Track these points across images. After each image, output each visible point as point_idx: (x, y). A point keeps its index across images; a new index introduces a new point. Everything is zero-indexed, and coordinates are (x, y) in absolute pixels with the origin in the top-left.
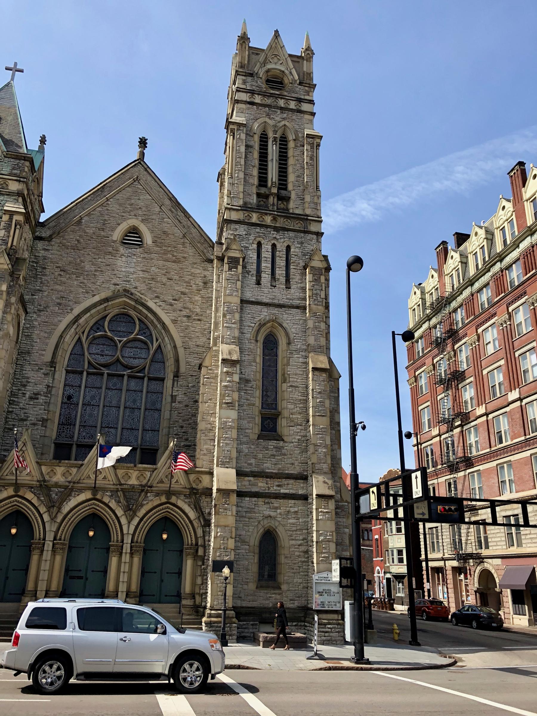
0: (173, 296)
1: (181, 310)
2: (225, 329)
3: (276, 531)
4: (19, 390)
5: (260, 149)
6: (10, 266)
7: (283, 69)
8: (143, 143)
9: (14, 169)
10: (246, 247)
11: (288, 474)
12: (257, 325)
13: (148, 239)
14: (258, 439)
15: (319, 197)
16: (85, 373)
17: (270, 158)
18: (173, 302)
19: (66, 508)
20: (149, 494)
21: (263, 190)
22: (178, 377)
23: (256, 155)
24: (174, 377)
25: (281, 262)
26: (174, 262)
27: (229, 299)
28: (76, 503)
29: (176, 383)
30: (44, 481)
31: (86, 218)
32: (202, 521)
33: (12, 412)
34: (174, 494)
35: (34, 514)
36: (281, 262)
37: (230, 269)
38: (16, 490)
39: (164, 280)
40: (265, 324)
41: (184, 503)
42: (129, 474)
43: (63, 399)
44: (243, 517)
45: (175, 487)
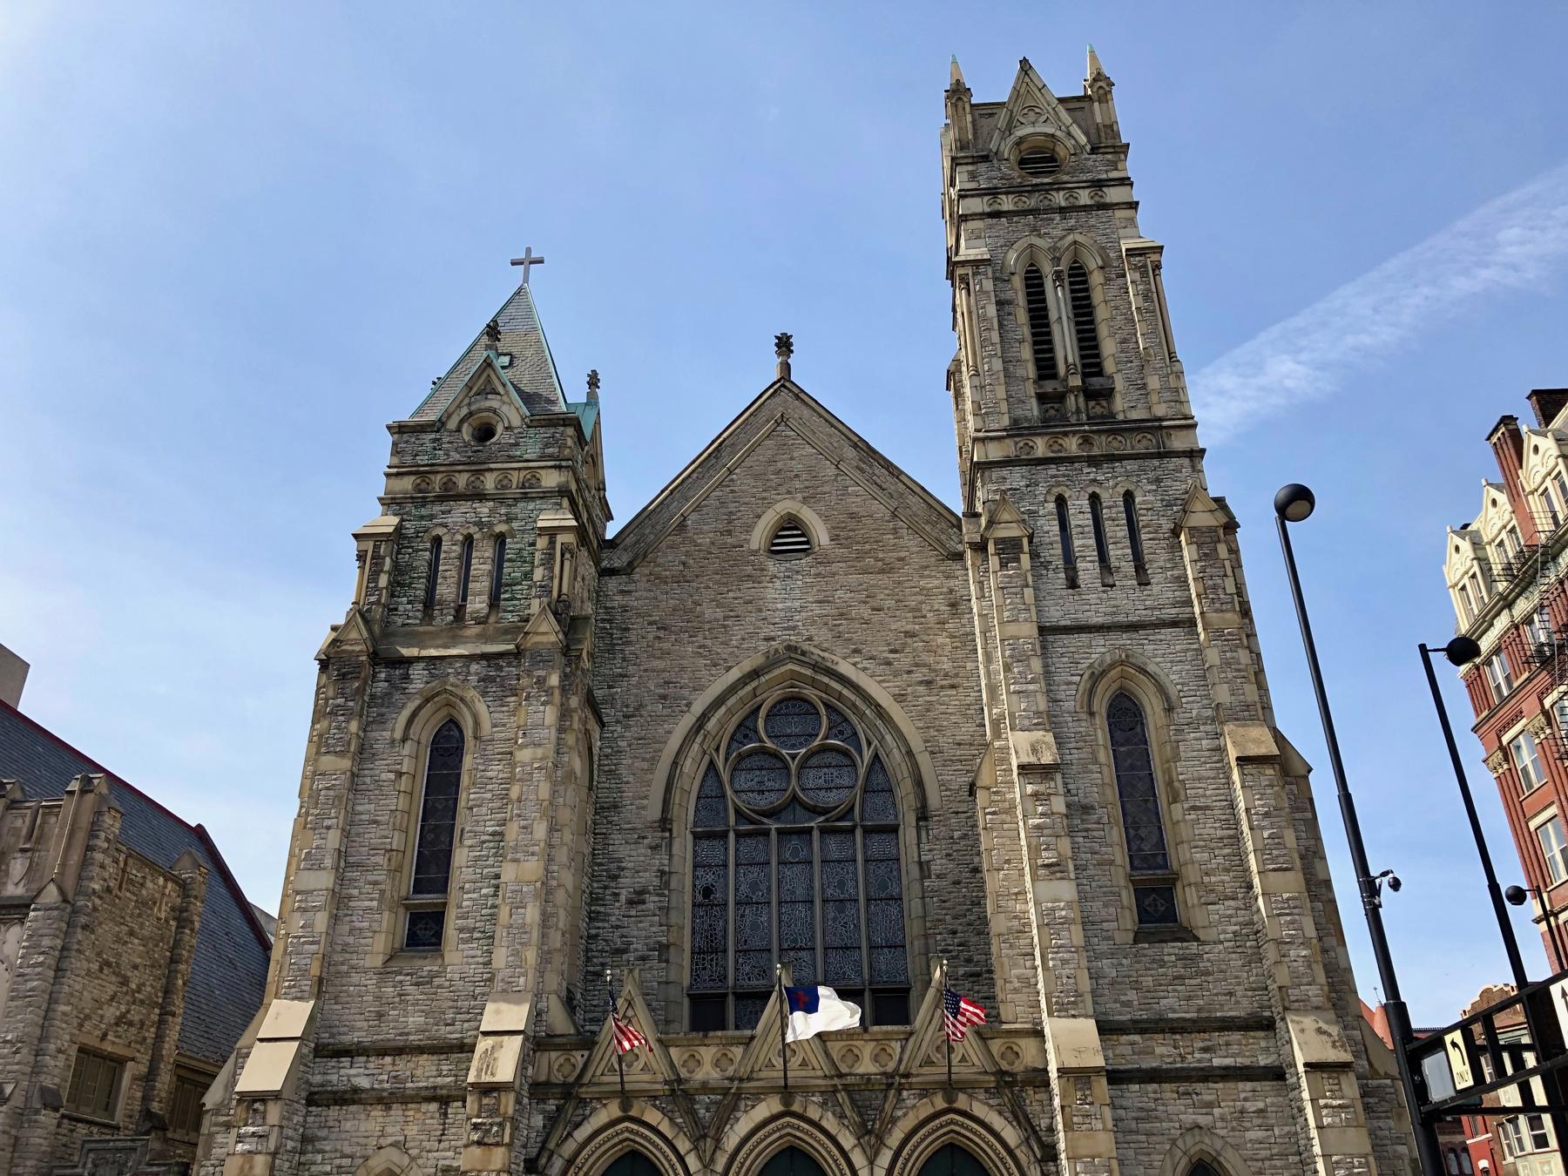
1: (909, 672)
2: (1015, 697)
3: (1219, 1163)
4: (606, 887)
5: (1029, 302)
6: (561, 636)
7: (1050, 130)
8: (784, 344)
9: (547, 446)
10: (1030, 512)
11: (1223, 1019)
12: (1086, 677)
13: (821, 534)
14: (1136, 941)
15: (1179, 374)
16: (732, 835)
17: (1053, 315)
19: (731, 1140)
20: (905, 1093)
21: (1049, 387)
22: (926, 819)
23: (1022, 316)
24: (918, 819)
25: (1116, 531)
26: (882, 571)
27: (1012, 629)
28: (752, 1125)
30: (679, 1081)
31: (694, 517)
33: (597, 935)
34: (960, 1090)
35: (666, 1157)
36: (1116, 531)
37: (1003, 565)
38: (625, 1106)
39: (865, 612)
40: (1103, 673)
42: (856, 1051)
43: (694, 897)
44: (1131, 1132)
45: (961, 1072)
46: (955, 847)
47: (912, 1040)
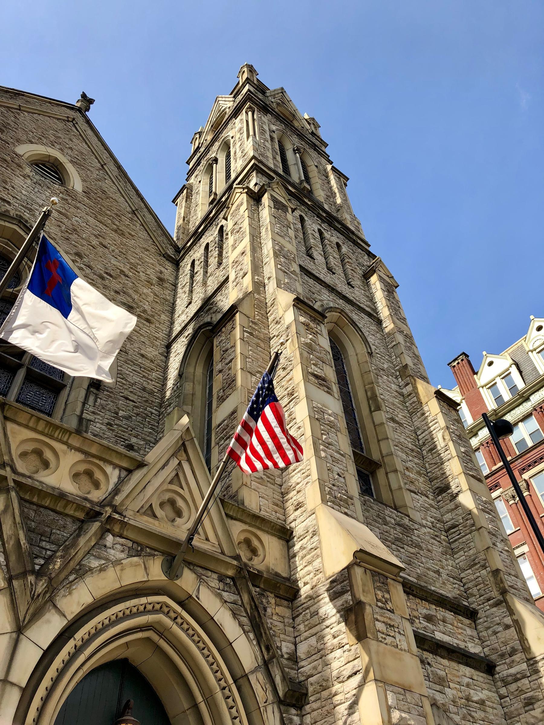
0: (106, 269)
18: (105, 275)
20: (110, 539)
29: (91, 399)
32: (278, 680)
34: (189, 564)
41: (217, 603)
46: (117, 422)
47: (137, 476)
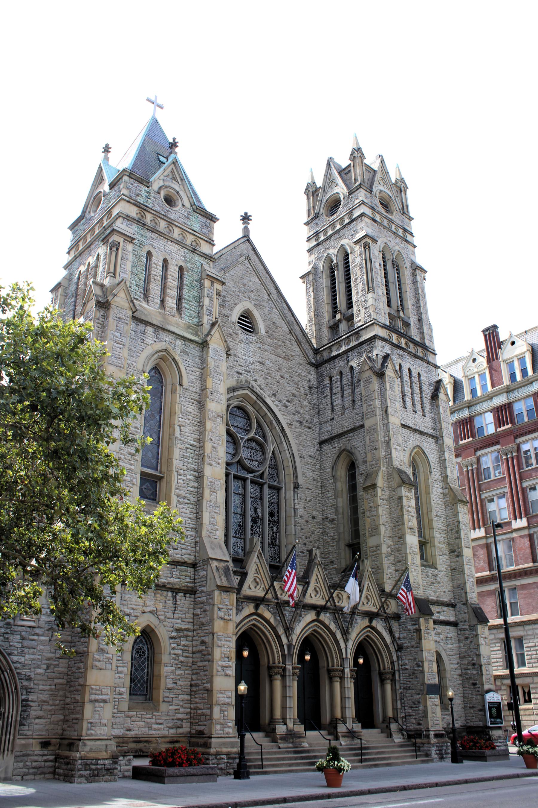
13: (262, 328)
24: (294, 488)
26: (285, 359)
46: (307, 505)
